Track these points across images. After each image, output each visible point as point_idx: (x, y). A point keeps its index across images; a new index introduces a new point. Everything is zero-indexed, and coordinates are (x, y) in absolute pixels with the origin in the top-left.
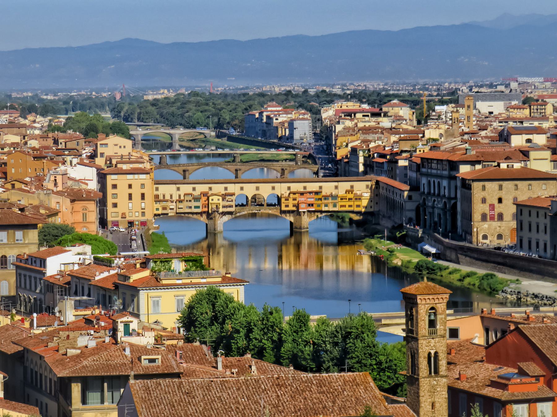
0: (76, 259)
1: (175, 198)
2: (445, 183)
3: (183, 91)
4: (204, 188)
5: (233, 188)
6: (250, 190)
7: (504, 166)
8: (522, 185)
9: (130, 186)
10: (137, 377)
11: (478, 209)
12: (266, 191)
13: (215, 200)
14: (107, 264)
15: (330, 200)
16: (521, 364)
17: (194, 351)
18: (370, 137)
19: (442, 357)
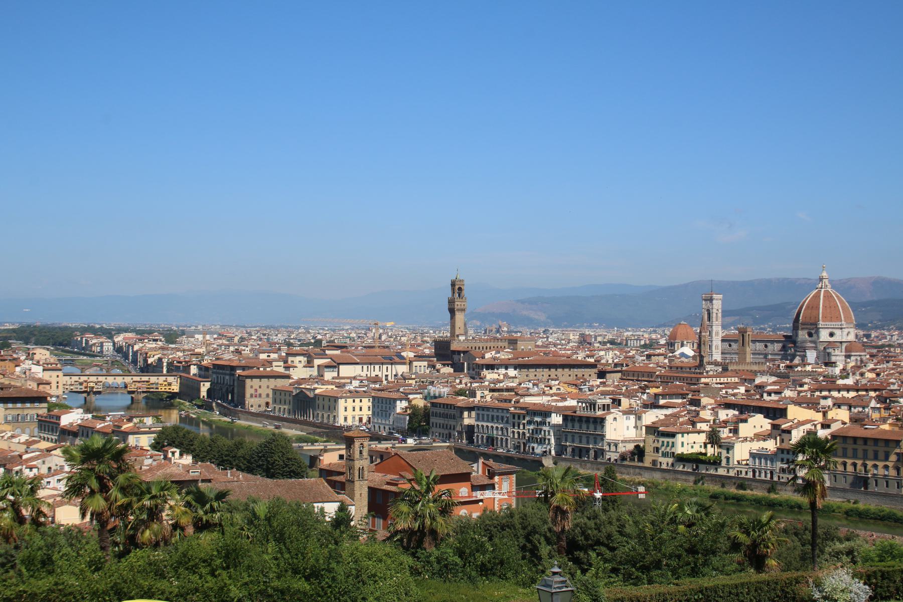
0: (79, 416)
1: (69, 383)
2: (227, 377)
3: (104, 326)
4: (85, 378)
5: (100, 378)
6: (110, 380)
7: (261, 369)
8: (272, 380)
10: (203, 481)
11: (249, 391)
12: (119, 380)
13: (92, 385)
14: (103, 419)
15: (154, 386)
16: (402, 473)
17: (207, 466)
18: (165, 352)
19: (365, 469)
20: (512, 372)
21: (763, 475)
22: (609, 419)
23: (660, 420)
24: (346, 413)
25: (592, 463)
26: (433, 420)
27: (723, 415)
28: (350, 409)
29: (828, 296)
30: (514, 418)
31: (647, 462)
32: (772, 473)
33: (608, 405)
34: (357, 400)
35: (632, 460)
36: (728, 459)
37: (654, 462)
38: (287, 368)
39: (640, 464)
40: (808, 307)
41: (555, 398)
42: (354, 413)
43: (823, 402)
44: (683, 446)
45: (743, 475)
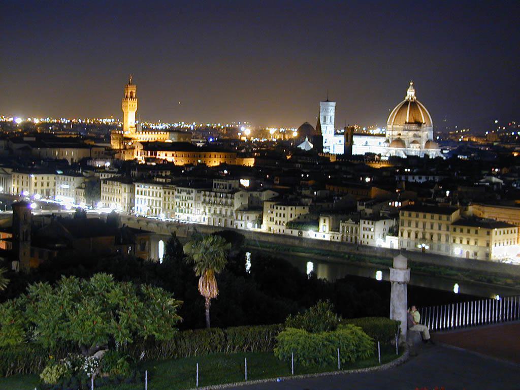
22: (237, 195)
30: (165, 193)
44: (291, 216)
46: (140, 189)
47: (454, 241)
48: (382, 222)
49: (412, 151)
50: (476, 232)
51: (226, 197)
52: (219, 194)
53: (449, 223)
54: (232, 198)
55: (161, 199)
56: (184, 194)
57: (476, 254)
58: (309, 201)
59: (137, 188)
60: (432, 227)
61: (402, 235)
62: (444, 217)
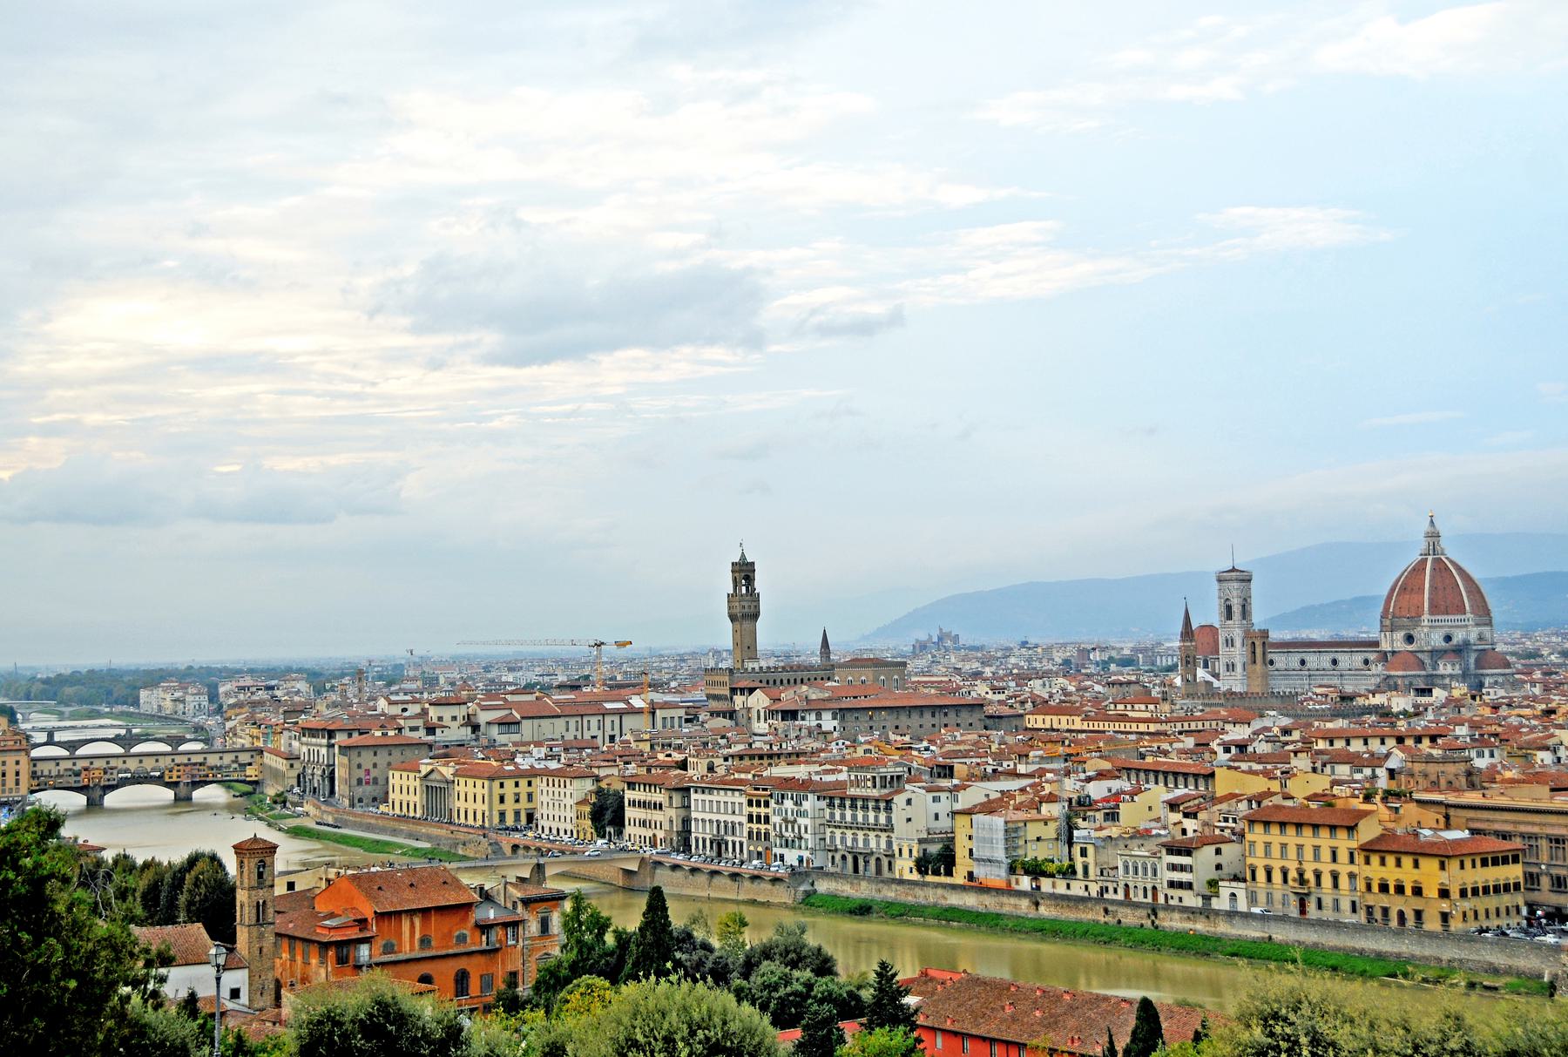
2: (324, 751)
9: (17, 763)
20: (828, 723)
21: (1141, 893)
22: (899, 800)
23: (989, 802)
24: (502, 807)
25: (870, 880)
26: (630, 813)
27: (1097, 790)
28: (509, 799)
29: (1440, 567)
31: (959, 878)
32: (1154, 888)
33: (899, 777)
34: (523, 782)
35: (936, 873)
36: (1086, 868)
37: (971, 876)
38: (431, 730)
39: (948, 880)
40: (1404, 589)
41: (828, 767)
42: (517, 806)
43: (1294, 762)
45: (1109, 896)
46: (699, 796)
47: (1369, 887)
48: (1212, 849)
49: (1443, 677)
50: (1416, 865)
51: (877, 809)
52: (859, 803)
53: (1354, 844)
54: (888, 809)
55: (744, 820)
56: (788, 804)
57: (1418, 914)
58: (1054, 810)
59: (693, 796)
60: (1317, 857)
61: (1254, 878)
62: (1342, 834)
